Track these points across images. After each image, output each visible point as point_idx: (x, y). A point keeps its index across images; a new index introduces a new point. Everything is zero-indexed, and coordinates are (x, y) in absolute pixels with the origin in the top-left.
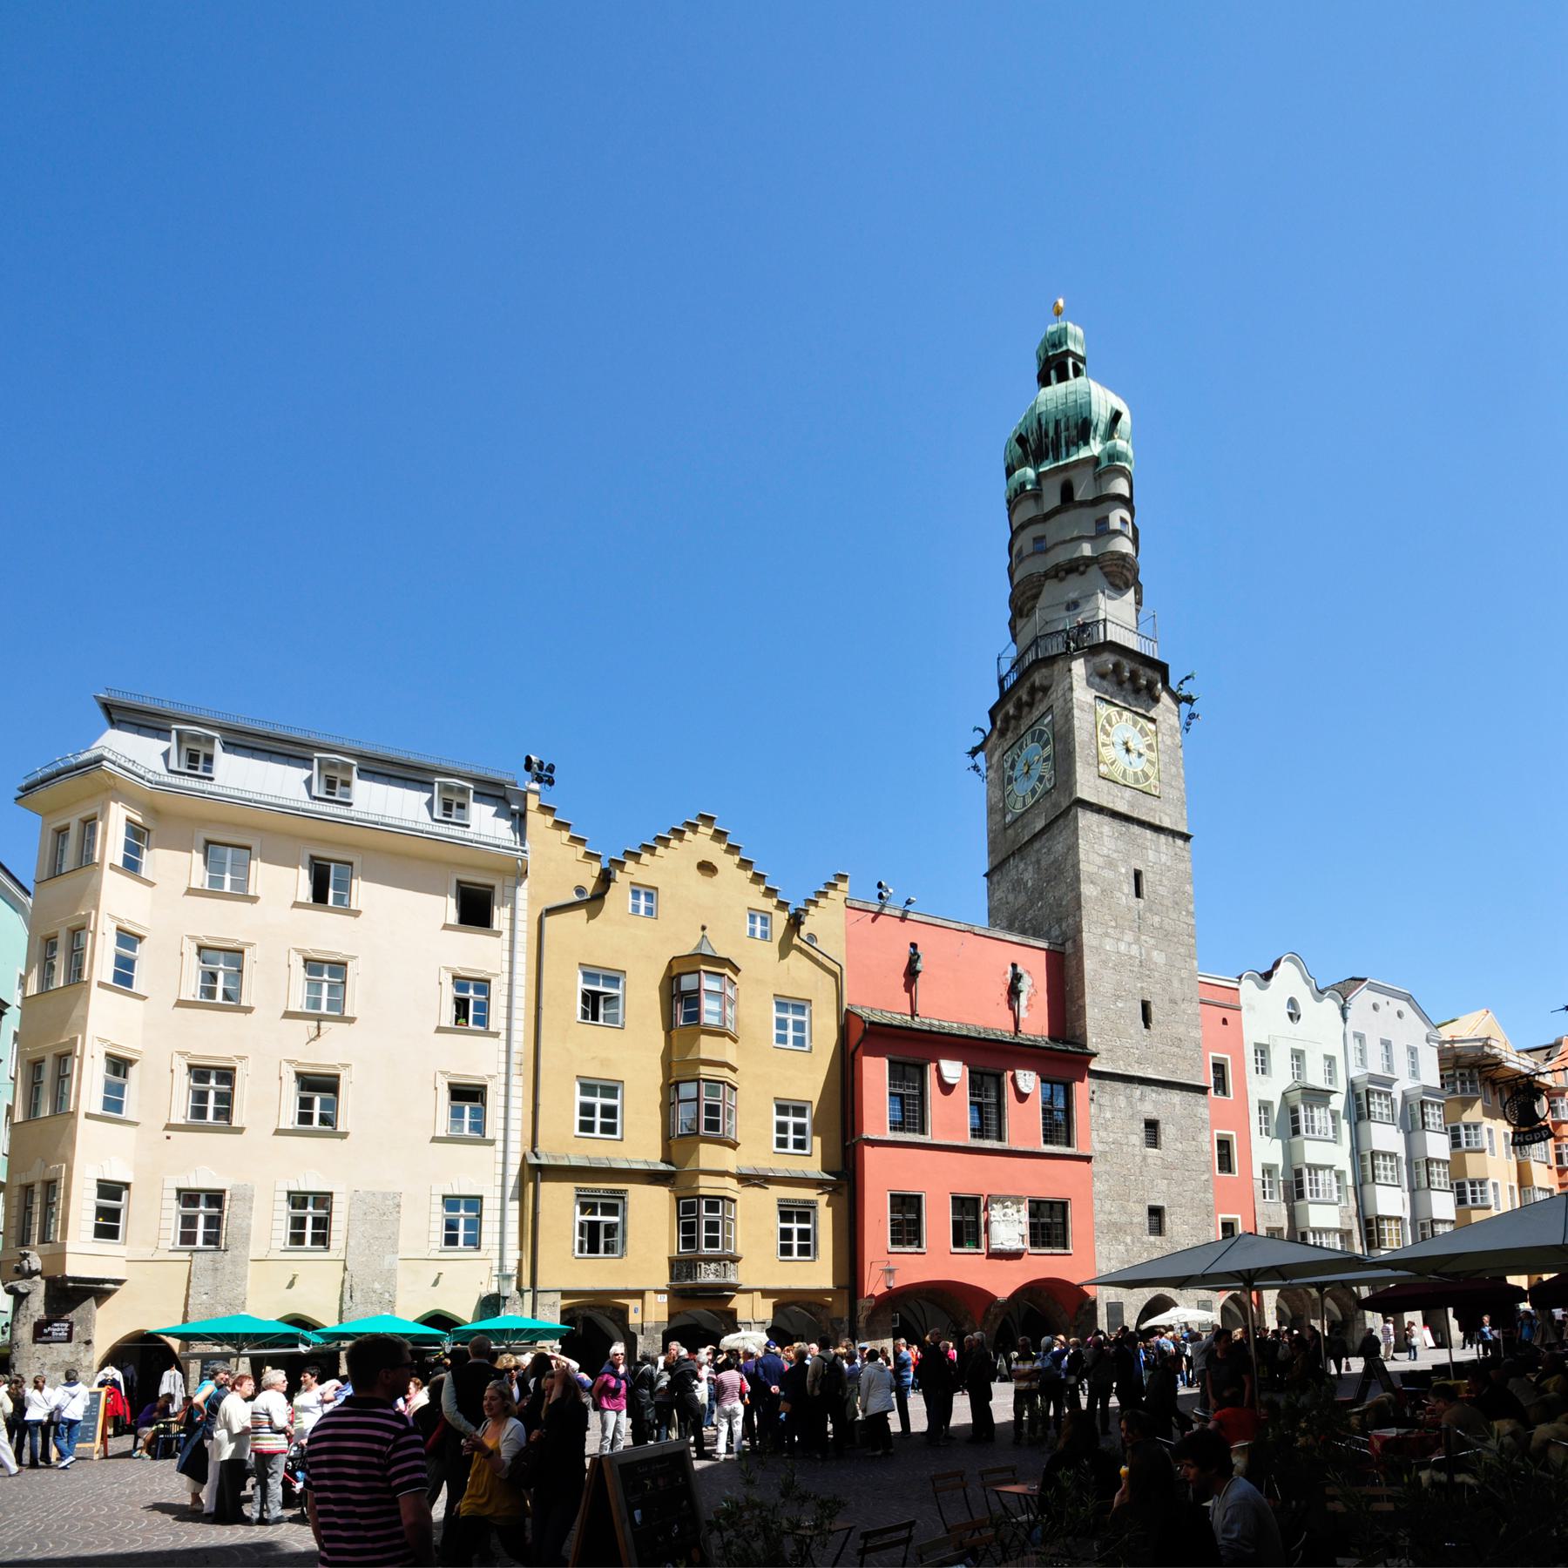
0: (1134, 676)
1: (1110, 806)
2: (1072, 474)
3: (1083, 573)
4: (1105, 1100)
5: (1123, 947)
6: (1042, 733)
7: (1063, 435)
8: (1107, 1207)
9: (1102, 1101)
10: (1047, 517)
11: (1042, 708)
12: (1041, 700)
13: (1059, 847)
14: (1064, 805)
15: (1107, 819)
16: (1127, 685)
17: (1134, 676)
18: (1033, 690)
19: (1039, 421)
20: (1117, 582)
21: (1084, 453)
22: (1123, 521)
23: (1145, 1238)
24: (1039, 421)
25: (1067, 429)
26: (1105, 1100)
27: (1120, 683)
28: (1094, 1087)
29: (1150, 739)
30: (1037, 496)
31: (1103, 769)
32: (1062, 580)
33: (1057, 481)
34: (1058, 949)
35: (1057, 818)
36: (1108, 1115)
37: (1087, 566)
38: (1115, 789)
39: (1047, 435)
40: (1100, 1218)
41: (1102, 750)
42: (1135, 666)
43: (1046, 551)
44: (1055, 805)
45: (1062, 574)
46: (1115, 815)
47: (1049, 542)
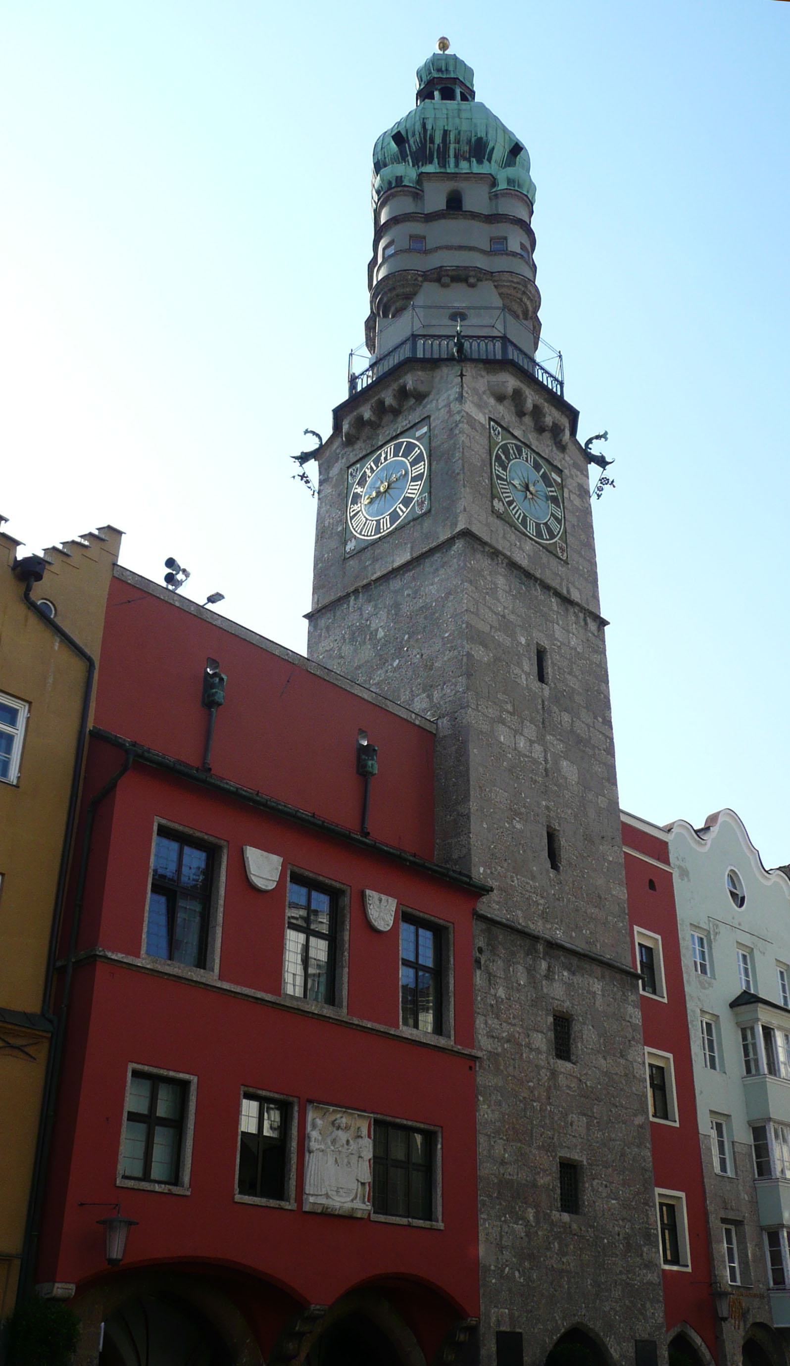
0: (537, 412)
1: (509, 554)
2: (462, 186)
3: (472, 286)
4: (497, 967)
5: (522, 743)
6: (410, 447)
7: (452, 146)
8: (498, 1150)
9: (493, 968)
10: (430, 218)
11: (414, 417)
12: (412, 409)
13: (433, 589)
14: (443, 537)
16: (527, 420)
18: (403, 394)
19: (424, 125)
20: (515, 307)
21: (476, 168)
22: (523, 246)
23: (556, 1215)
24: (424, 125)
25: (458, 142)
26: (497, 967)
27: (520, 414)
28: (481, 942)
29: (552, 491)
30: (417, 194)
31: (498, 505)
32: (445, 286)
33: (448, 186)
34: (428, 726)
35: (431, 552)
36: (501, 993)
37: (479, 280)
38: (512, 537)
39: (432, 141)
40: (486, 1169)
42: (540, 401)
43: (426, 252)
45: (446, 280)
46: (513, 565)
47: (430, 244)
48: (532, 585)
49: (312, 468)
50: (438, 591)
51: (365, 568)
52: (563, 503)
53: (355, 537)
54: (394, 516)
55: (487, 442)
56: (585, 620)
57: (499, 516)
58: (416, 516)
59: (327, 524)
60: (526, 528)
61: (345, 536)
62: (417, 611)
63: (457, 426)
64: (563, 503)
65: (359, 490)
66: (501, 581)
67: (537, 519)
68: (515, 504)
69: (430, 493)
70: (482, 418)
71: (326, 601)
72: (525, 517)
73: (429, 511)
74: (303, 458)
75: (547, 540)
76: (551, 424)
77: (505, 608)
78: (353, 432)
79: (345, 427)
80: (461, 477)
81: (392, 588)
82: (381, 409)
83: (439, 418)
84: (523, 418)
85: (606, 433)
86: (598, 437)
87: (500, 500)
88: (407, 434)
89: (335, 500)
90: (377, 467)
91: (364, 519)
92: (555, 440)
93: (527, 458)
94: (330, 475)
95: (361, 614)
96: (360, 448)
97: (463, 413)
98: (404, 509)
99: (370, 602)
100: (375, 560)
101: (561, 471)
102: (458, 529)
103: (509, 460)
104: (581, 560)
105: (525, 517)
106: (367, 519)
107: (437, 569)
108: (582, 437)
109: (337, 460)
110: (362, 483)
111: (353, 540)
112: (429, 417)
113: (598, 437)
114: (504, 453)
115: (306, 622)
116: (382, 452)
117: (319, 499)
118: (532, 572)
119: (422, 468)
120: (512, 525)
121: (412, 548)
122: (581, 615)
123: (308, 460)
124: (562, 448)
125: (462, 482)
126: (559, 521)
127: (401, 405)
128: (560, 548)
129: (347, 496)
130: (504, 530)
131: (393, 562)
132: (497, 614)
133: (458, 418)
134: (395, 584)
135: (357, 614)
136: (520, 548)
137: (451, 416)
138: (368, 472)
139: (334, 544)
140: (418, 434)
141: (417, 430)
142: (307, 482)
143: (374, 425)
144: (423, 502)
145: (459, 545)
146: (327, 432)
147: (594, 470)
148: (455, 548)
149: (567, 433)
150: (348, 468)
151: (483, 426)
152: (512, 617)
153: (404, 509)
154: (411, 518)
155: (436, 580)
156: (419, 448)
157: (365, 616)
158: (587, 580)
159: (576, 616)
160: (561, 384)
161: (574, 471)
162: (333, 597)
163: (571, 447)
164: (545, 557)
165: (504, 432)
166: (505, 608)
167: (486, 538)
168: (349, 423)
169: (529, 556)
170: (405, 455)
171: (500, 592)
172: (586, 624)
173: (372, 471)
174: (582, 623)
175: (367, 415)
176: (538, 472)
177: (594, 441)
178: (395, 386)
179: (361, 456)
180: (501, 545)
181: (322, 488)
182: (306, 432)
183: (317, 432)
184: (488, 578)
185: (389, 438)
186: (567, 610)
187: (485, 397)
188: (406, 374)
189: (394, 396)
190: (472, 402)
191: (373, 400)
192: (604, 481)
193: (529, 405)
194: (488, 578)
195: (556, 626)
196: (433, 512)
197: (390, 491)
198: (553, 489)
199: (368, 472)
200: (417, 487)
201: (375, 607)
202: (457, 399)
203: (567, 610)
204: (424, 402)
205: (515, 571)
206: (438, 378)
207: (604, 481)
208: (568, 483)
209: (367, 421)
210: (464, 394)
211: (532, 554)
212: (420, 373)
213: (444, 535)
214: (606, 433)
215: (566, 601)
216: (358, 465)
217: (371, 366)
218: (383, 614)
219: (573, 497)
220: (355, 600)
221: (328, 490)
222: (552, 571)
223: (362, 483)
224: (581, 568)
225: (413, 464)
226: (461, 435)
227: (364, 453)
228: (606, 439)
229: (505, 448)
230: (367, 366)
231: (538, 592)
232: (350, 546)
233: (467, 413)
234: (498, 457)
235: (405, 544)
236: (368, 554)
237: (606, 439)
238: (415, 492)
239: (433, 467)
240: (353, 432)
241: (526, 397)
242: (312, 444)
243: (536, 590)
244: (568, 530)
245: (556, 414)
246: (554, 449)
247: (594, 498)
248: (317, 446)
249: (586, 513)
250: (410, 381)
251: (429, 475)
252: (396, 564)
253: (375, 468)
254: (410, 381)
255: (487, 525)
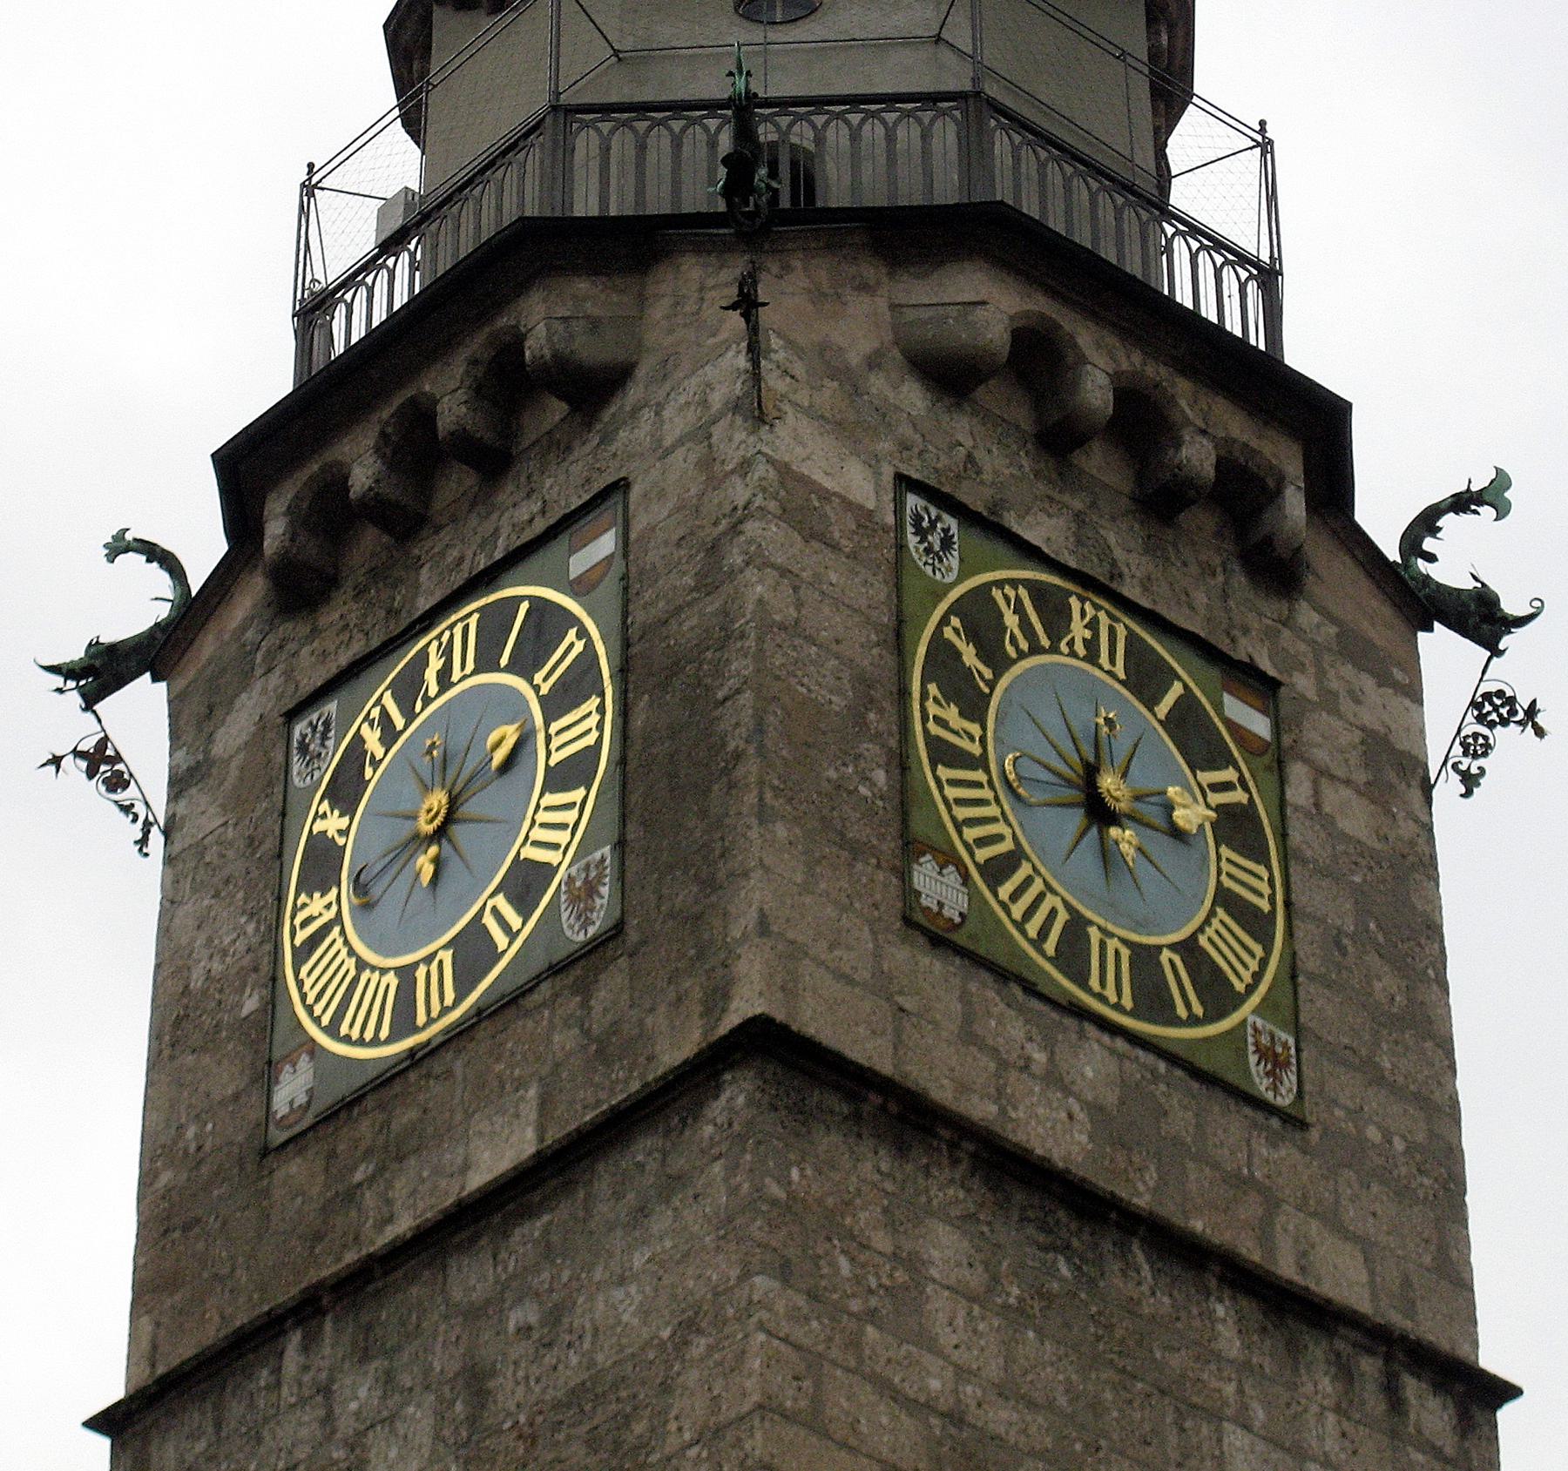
0: (1140, 422)
1: (981, 1110)
6: (547, 624)
11: (564, 486)
12: (557, 446)
13: (627, 1302)
15: (948, 1189)
16: (1098, 461)
17: (1140, 422)
18: (510, 381)
27: (1058, 440)
31: (936, 887)
38: (1010, 1026)
41: (943, 787)
44: (602, 1050)
46: (1005, 1167)
48: (1107, 1246)
49: (140, 714)
50: (645, 1313)
51: (351, 1196)
52: (1283, 836)
53: (313, 1048)
54: (473, 951)
55: (880, 590)
56: (1392, 1391)
57: (938, 937)
58: (560, 954)
59: (197, 980)
60: (1082, 980)
61: (267, 1038)
62: (557, 1406)
63: (735, 530)
64: (1283, 836)
65: (333, 823)
66: (945, 1248)
67: (1139, 926)
68: (1025, 870)
69: (621, 845)
70: (859, 483)
71: (184, 1350)
72: (1077, 925)
73: (617, 931)
74: (100, 672)
75: (1193, 1021)
76: (1208, 470)
77: (963, 1373)
78: (311, 549)
79: (275, 530)
80: (750, 769)
81: (457, 1294)
82: (418, 449)
83: (663, 492)
84: (1079, 458)
85: (1501, 481)
86: (1463, 502)
87: (947, 858)
88: (535, 563)
89: (231, 871)
90: (410, 716)
91: (351, 963)
92: (1241, 534)
93: (1092, 645)
94: (217, 750)
95: (328, 1419)
96: (341, 629)
97: (761, 469)
98: (515, 921)
99: (365, 1357)
100: (395, 1154)
101: (1272, 685)
102: (732, 1020)
103: (997, 661)
104: (1375, 1100)
105: (1077, 925)
106: (361, 965)
107: (642, 1212)
108: (1381, 515)
109: (245, 679)
110: (344, 792)
111: (304, 1062)
112: (621, 486)
113: (1463, 502)
114: (973, 635)
115: (101, 1445)
116: (429, 642)
117: (169, 860)
118: (1103, 1182)
119: (588, 726)
120: (1008, 975)
121: (545, 1103)
122: (1369, 1366)
123: (120, 682)
124: (1278, 573)
125: (751, 798)
126: (1256, 923)
127: (508, 432)
128: (1264, 1054)
129: (280, 855)
130: (965, 997)
131: (466, 1167)
132: (920, 1407)
133: (739, 492)
134: (471, 1276)
135: (311, 1415)
136: (1054, 1079)
137: (714, 482)
138: (372, 738)
139: (225, 1078)
140: (580, 563)
141: (572, 551)
142: (117, 783)
143: (404, 522)
144: (591, 889)
145: (737, 1095)
146: (203, 546)
147: (1445, 658)
148: (717, 1109)
149: (1294, 504)
150: (292, 715)
151: (865, 517)
152: (1001, 1418)
153: (515, 921)
154: (539, 963)
155: (638, 1260)
156: (583, 633)
157: (346, 1425)
158: (1402, 1193)
159: (1345, 1373)
160: (1268, 277)
161: (1343, 674)
162: (208, 1332)
163: (1330, 570)
164: (1181, 1109)
165: (977, 540)
166: (963, 1373)
167: (867, 1047)
168: (289, 511)
169: (1095, 1109)
170: (524, 665)
171: (939, 1304)
172: (1396, 1404)
173: (389, 735)
174: (1375, 1403)
175: (363, 475)
176: (1151, 703)
177: (1448, 521)
178: (476, 345)
179: (344, 659)
180: (943, 1074)
181: (181, 808)
182: (118, 547)
183: (166, 544)
184: (882, 1241)
185: (458, 579)
186: (1294, 1350)
187: (877, 383)
188: (522, 288)
189: (478, 391)
190: (810, 412)
191: (386, 414)
192: (1495, 708)
193: (1095, 390)
194: (882, 1241)
195: (1235, 1438)
196: (633, 936)
197: (456, 830)
198: (1229, 775)
199: (372, 738)
200: (570, 816)
201: (388, 1380)
202: (736, 407)
203: (1294, 1350)
204: (606, 415)
205: (1019, 1197)
206: (666, 302)
207: (1495, 708)
208: (1310, 735)
209: (362, 501)
210: (774, 382)
211: (1111, 1098)
212: (582, 285)
213: (676, 1046)
214: (1501, 481)
215: (1290, 1309)
216: (331, 707)
217: (390, 245)
218: (419, 1418)
219: (1334, 797)
220: (305, 1348)
221: (206, 816)
222: (1202, 1177)
223: (344, 792)
224: (1373, 1133)
225: (556, 705)
226: (751, 574)
227: (357, 648)
228: (1502, 511)
229: (978, 616)
230: (366, 243)
231: (1139, 1281)
232: (292, 1089)
233: (784, 470)
234: (942, 654)
235: (520, 1084)
236: (364, 1128)
237: (1502, 511)
238: (562, 837)
239: (638, 722)
240: (311, 549)
241: (1082, 360)
242: (136, 604)
243: (1129, 1267)
244: (1310, 962)
245: (1236, 425)
246: (1240, 580)
247: (1447, 790)
248: (163, 611)
249: (1415, 864)
250: (544, 320)
251: (621, 761)
252: (476, 1180)
253: (399, 722)
254: (544, 320)
255: (883, 985)
